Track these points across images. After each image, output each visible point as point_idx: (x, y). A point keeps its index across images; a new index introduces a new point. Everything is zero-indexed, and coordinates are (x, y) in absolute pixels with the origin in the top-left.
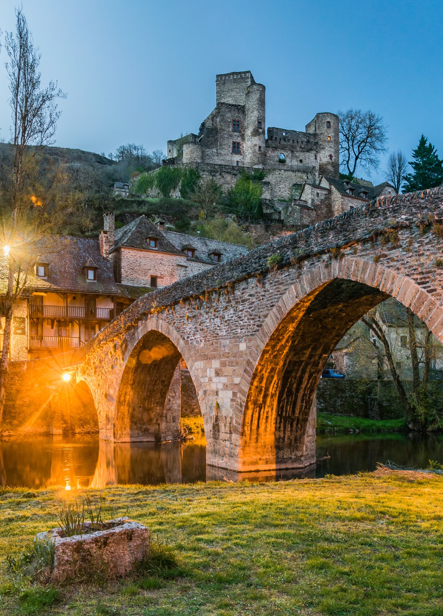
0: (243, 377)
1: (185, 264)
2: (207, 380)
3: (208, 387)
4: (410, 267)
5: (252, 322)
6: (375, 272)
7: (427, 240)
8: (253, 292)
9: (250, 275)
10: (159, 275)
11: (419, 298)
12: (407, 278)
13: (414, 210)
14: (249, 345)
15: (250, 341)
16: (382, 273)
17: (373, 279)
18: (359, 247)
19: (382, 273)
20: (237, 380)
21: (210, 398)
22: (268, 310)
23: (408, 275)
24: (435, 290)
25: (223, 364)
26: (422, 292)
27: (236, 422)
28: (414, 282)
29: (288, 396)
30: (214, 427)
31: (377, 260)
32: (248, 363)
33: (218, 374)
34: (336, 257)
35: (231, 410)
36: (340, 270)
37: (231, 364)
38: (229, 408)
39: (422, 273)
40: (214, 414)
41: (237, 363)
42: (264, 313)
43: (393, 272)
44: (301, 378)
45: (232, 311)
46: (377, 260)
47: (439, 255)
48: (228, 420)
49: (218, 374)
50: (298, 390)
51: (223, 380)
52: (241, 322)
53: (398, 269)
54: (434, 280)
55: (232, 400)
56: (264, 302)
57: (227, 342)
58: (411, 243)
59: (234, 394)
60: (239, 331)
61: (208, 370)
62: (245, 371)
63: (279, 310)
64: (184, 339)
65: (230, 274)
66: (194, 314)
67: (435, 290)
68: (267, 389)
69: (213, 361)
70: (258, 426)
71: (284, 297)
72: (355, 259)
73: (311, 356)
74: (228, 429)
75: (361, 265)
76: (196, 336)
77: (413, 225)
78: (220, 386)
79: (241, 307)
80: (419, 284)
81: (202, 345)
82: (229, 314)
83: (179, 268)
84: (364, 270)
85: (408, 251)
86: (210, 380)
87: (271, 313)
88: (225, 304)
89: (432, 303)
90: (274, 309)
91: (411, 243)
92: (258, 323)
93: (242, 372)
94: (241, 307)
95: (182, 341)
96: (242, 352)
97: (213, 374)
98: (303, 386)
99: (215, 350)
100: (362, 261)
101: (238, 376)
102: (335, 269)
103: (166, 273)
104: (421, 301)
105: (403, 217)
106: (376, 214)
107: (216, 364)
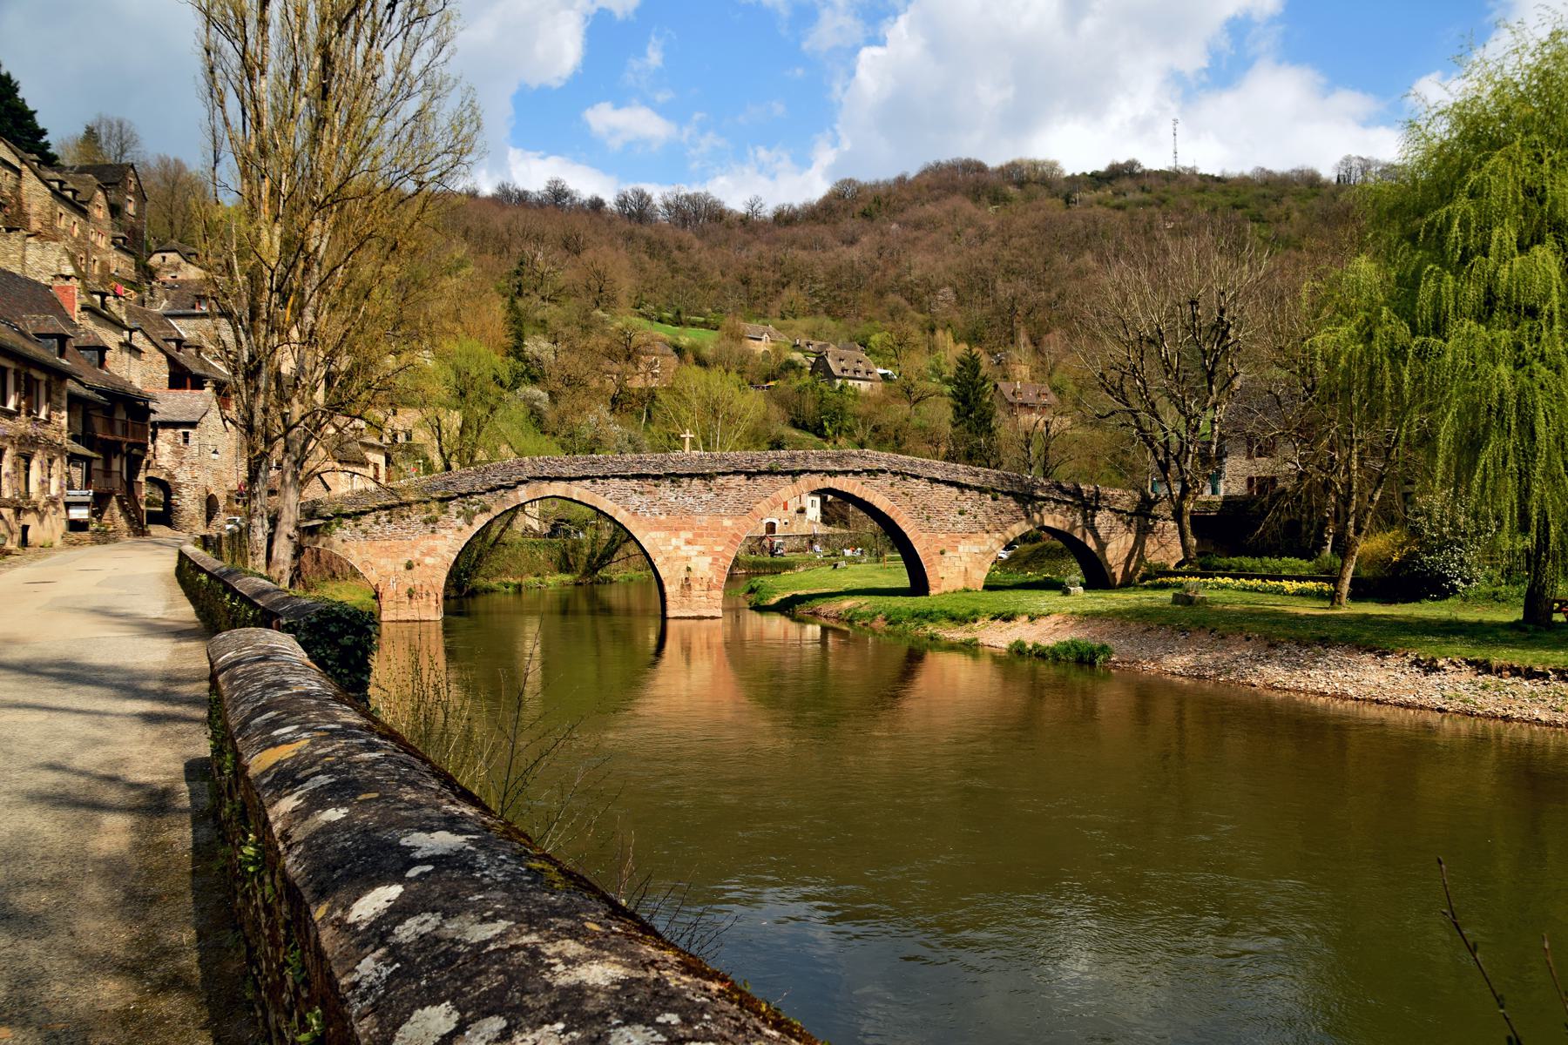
20: (719, 549)
25: (695, 535)
30: (682, 586)
33: (688, 542)
37: (711, 535)
40: (683, 577)
41: (719, 536)
59: (716, 560)
81: (663, 517)
95: (623, 512)
97: (681, 543)
104: (893, 509)
107: (689, 535)
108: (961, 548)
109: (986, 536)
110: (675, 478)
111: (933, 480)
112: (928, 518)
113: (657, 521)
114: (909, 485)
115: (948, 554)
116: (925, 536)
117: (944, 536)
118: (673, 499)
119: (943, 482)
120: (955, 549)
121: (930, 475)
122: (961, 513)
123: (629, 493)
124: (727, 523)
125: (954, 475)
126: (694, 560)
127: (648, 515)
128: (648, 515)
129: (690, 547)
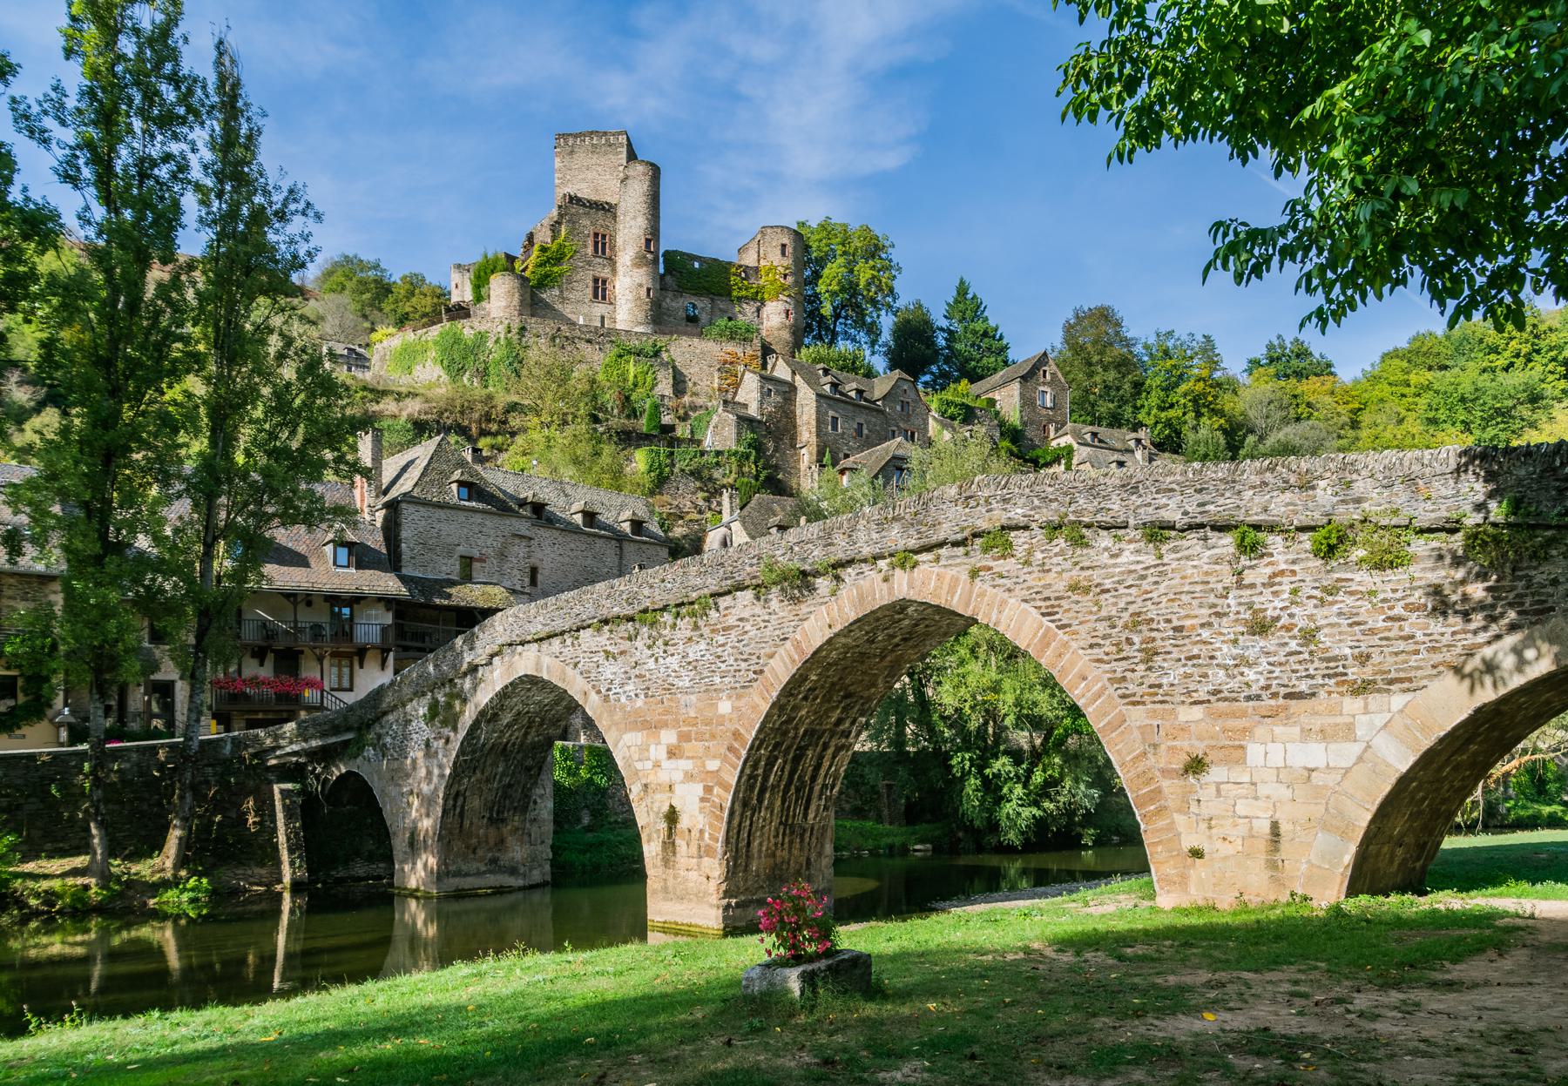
0: (725, 759)
1: (527, 533)
2: (649, 765)
3: (651, 779)
4: (1029, 588)
5: (744, 665)
6: (971, 592)
7: (1057, 550)
8: (746, 614)
9: (740, 587)
10: (477, 555)
11: (1044, 636)
12: (1024, 605)
13: (1036, 502)
14: (737, 704)
15: (739, 697)
16: (982, 594)
17: (968, 604)
18: (943, 551)
19: (982, 594)
20: (713, 765)
21: (658, 796)
22: (776, 646)
23: (1025, 601)
24: (1069, 625)
25: (684, 737)
26: (1048, 629)
27: (712, 838)
28: (1034, 611)
29: (798, 790)
31: (974, 574)
32: (736, 735)
33: (672, 753)
34: (903, 566)
35: (701, 818)
36: (911, 586)
38: (697, 812)
39: (1048, 599)
41: (713, 736)
42: (768, 650)
43: (1001, 594)
44: (821, 757)
45: (703, 646)
46: (974, 574)
47: (1074, 573)
48: (695, 833)
49: (672, 753)
50: (814, 778)
51: (685, 764)
52: (723, 666)
53: (1009, 590)
54: (1068, 610)
55: (702, 800)
56: (768, 632)
57: (693, 697)
58: (1030, 553)
59: (708, 789)
60: (717, 680)
61: (652, 748)
62: (730, 749)
63: (797, 646)
64: (599, 692)
65: (698, 581)
66: (622, 648)
67: (1069, 625)
68: (766, 778)
69: (663, 732)
70: (749, 844)
71: (806, 624)
72: (936, 570)
73: (839, 721)
74: (694, 850)
75: (947, 580)
76: (627, 688)
77: (1034, 525)
78: (678, 776)
79: (721, 640)
80: (1043, 615)
81: (639, 703)
82: (696, 651)
83: (517, 541)
84: (952, 591)
85: (1027, 563)
86: (657, 765)
87: (781, 650)
88: (689, 634)
89: (1065, 645)
90: (788, 644)
91: (1030, 553)
92: (757, 668)
93: (723, 750)
94: (721, 640)
95: (594, 696)
96: (723, 716)
97: (663, 754)
98: (822, 772)
99: (666, 712)
100: (950, 572)
101: (714, 757)
102: (900, 585)
103: (490, 551)
105: (1019, 511)
106: (972, 503)
107: (669, 737)
108: (1254, 752)
109: (1352, 704)
110: (647, 616)
111: (1157, 532)
112: (1150, 654)
113: (637, 711)
114: (1086, 556)
115: (1216, 774)
116: (1137, 715)
117: (1197, 712)
118: (651, 664)
119: (1191, 527)
120: (1235, 756)
121: (1148, 514)
122: (1260, 627)
123: (600, 658)
124: (725, 707)
125: (1229, 501)
126: (678, 789)
127: (623, 699)
128: (623, 699)
129: (673, 763)
